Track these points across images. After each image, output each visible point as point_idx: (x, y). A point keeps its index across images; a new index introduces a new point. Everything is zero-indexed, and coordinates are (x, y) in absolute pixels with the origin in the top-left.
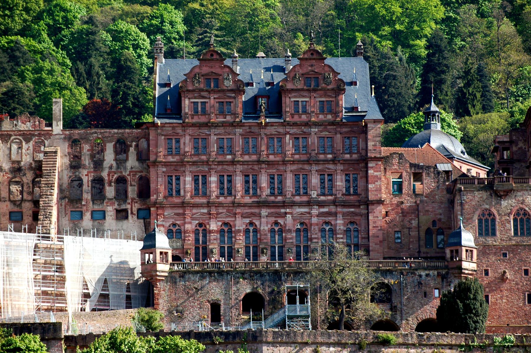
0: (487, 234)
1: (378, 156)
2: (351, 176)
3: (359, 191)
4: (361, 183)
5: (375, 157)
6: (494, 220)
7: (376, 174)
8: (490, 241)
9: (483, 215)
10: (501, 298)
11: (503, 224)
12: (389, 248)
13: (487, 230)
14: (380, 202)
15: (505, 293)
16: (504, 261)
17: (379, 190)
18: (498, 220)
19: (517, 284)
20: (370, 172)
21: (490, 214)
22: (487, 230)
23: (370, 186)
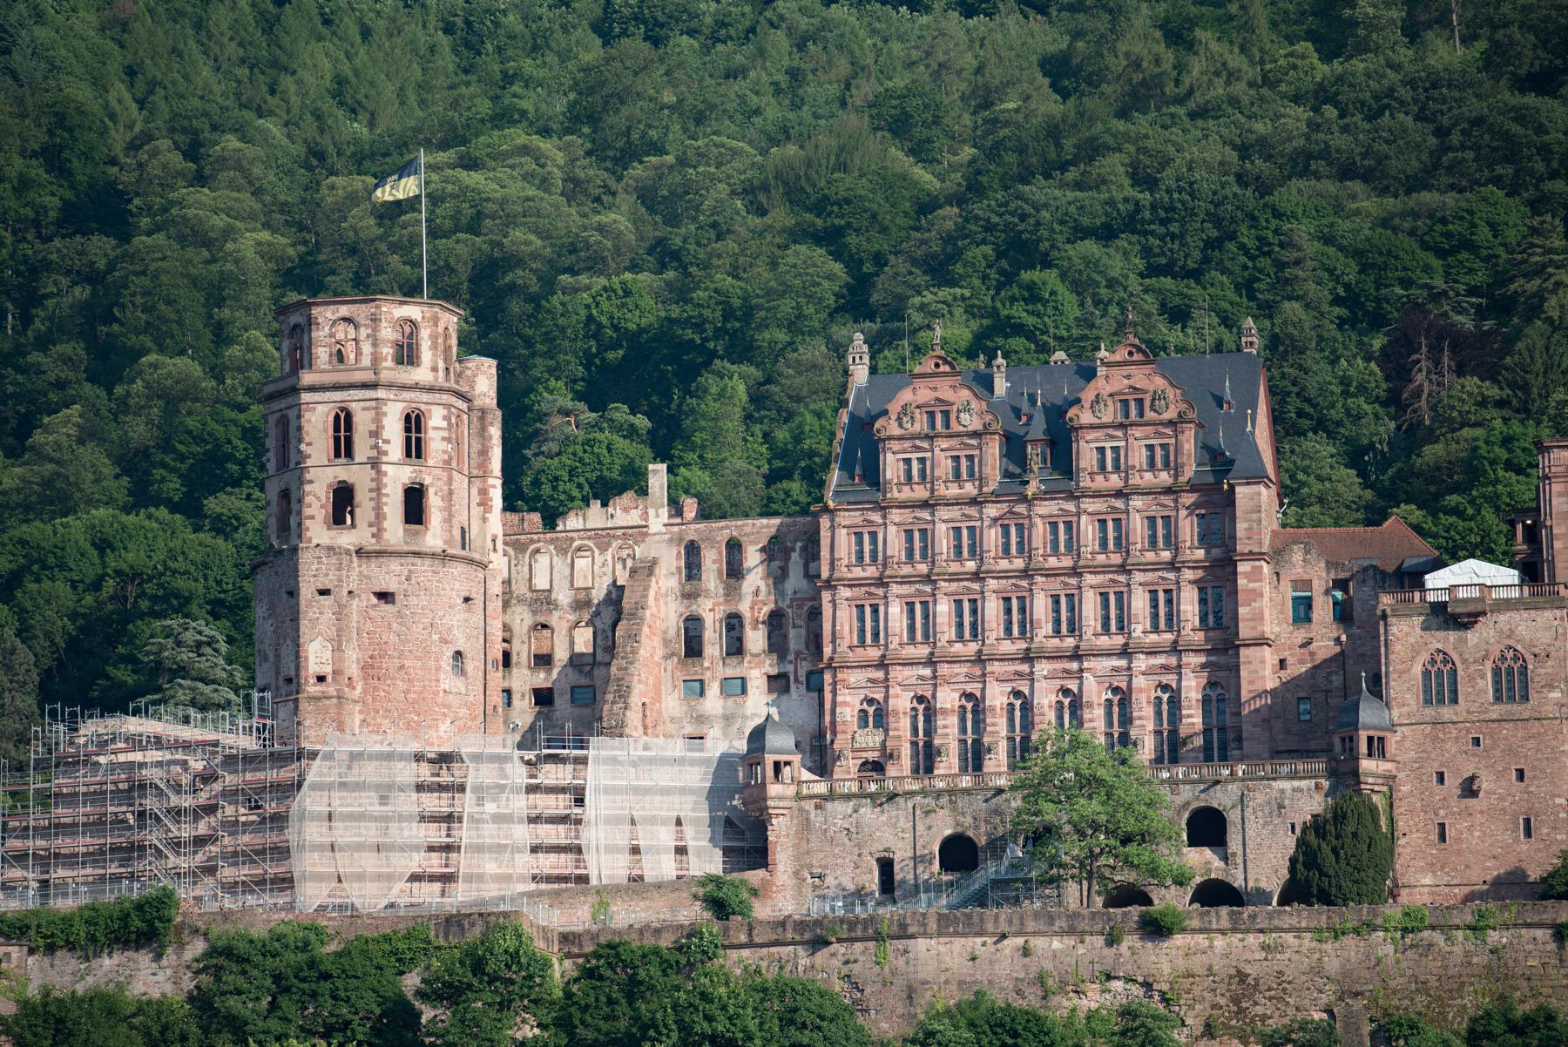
0: (1441, 701)
1: (1256, 550)
2: (1210, 591)
6: (1454, 672)
7: (1251, 585)
8: (1447, 712)
9: (1433, 661)
10: (1470, 828)
11: (1471, 679)
13: (1440, 693)
14: (1261, 642)
15: (1479, 818)
17: (1259, 618)
18: (1460, 673)
20: (1241, 582)
21: (1447, 660)
22: (1440, 693)
23: (1241, 610)
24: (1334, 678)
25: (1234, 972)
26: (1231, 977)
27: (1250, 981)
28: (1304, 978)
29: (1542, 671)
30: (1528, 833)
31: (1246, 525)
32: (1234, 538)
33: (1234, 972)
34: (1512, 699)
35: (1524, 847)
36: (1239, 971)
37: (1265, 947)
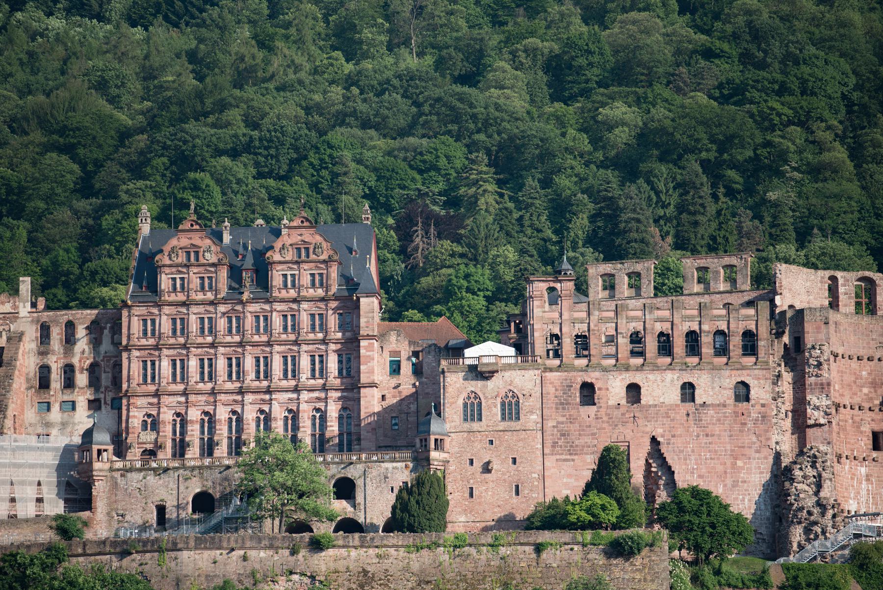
2: (344, 356)
3: (352, 373)
4: (353, 364)
5: (368, 335)
6: (480, 404)
8: (476, 426)
9: (469, 398)
11: (489, 408)
12: (385, 436)
14: (373, 385)
15: (491, 485)
16: (490, 450)
17: (372, 372)
19: (503, 474)
23: (362, 367)
24: (412, 406)
25: (361, 570)
26: (359, 573)
27: (370, 575)
28: (399, 573)
29: (527, 404)
30: (517, 493)
31: (366, 320)
32: (359, 327)
33: (361, 570)
34: (511, 419)
35: (515, 501)
36: (364, 570)
37: (379, 556)
